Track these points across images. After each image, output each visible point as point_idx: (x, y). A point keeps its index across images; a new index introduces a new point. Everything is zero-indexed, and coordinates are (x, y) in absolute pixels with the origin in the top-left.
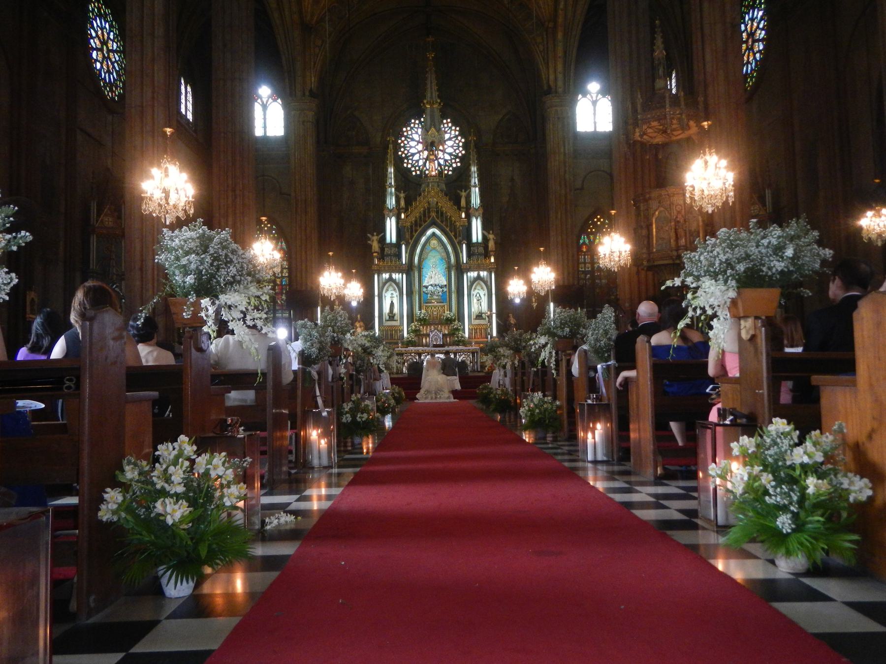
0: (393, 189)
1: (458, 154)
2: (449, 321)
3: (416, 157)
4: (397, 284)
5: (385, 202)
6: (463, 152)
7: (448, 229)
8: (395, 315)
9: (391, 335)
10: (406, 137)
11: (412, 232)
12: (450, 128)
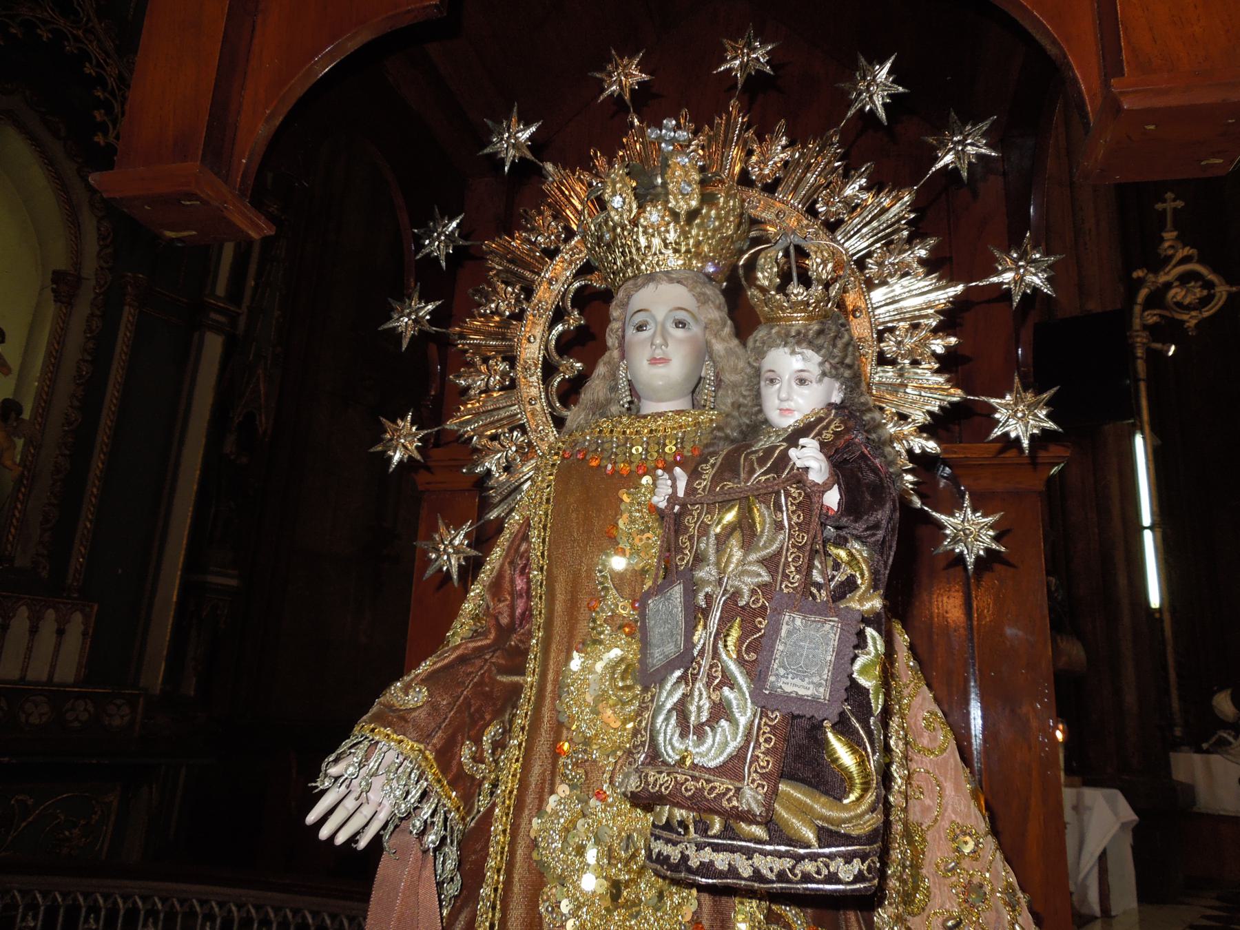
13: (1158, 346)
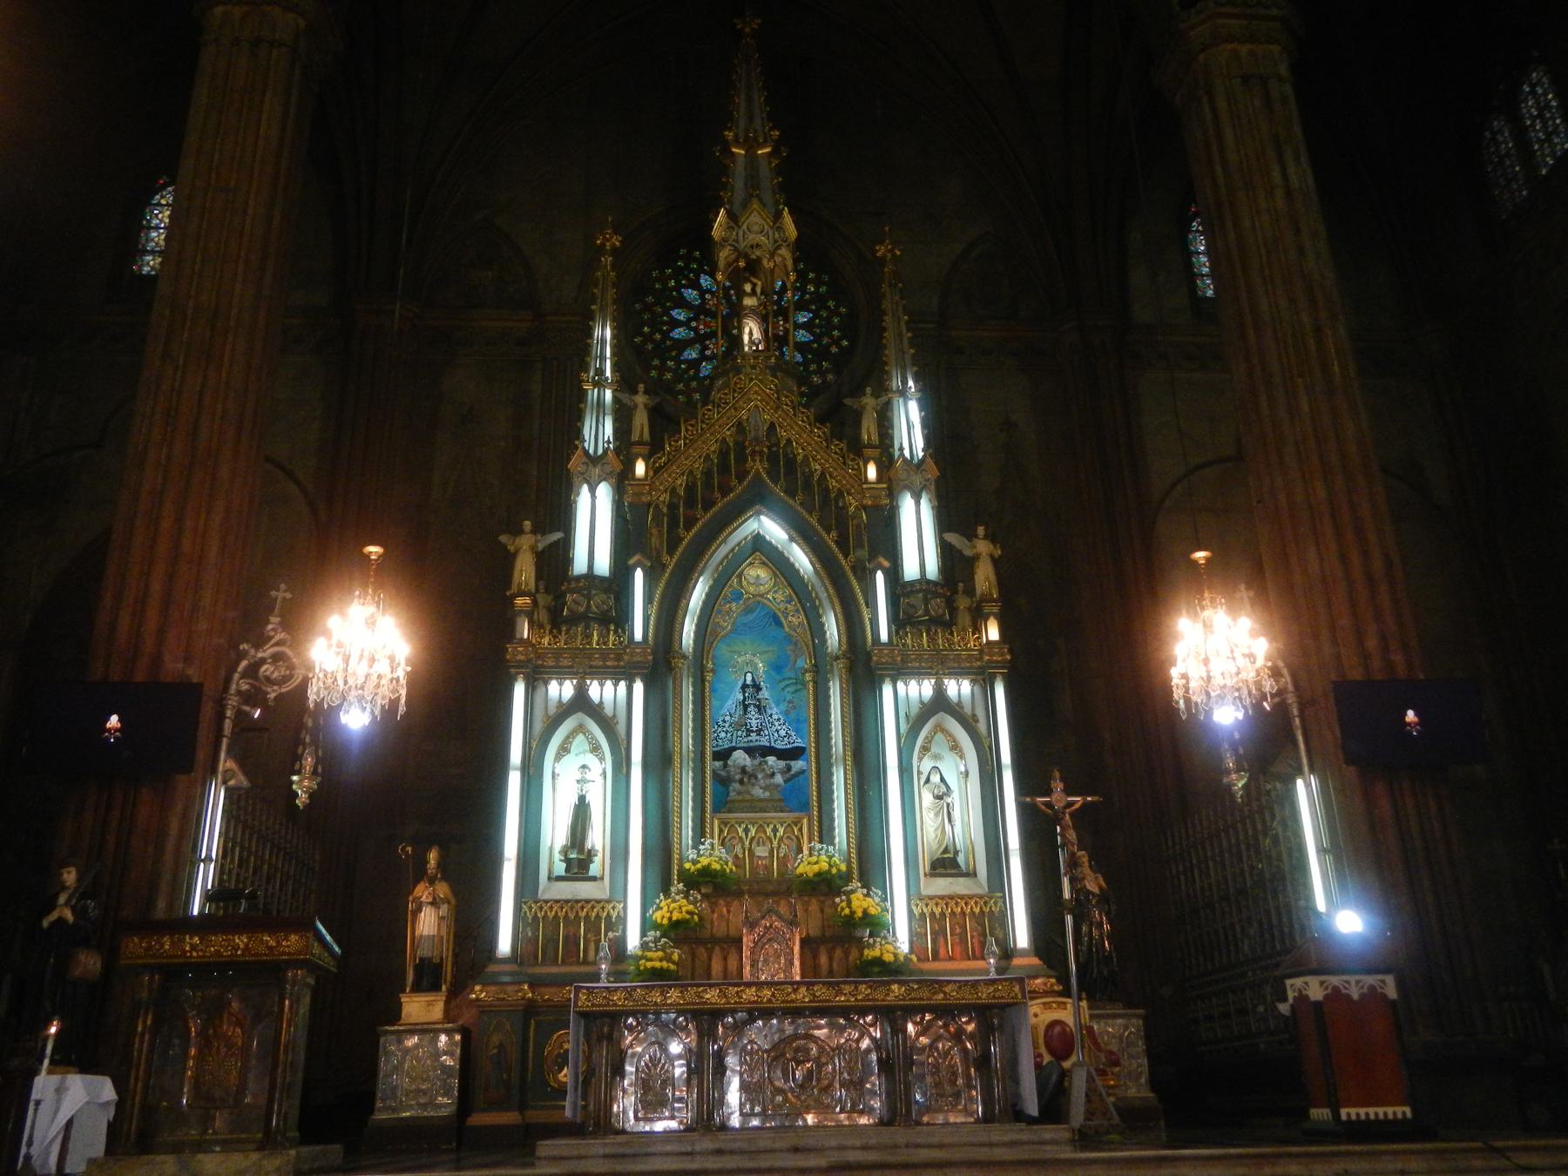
0: (608, 395)
1: (829, 345)
2: (826, 886)
3: (691, 354)
4: (607, 724)
5: (578, 434)
8: (590, 855)
9: (572, 941)
11: (673, 524)
13: (247, 708)
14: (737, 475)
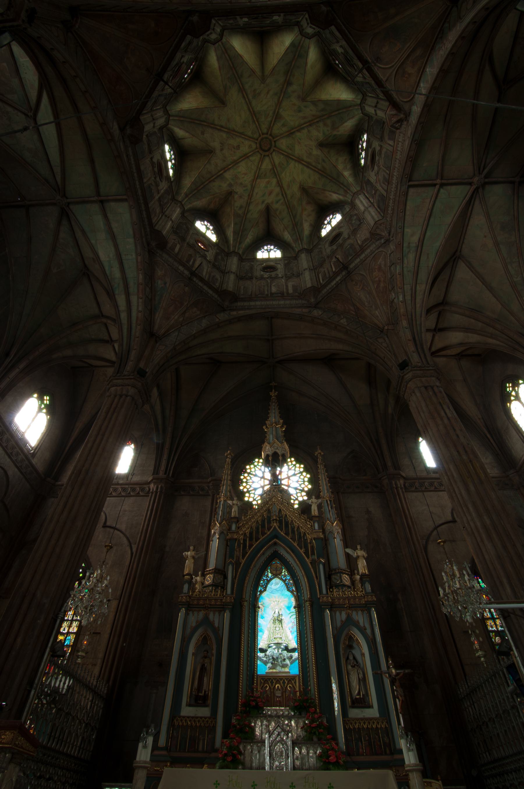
6: (310, 486)
7: (296, 544)
10: (249, 474)
12: (295, 465)
14: (267, 529)
